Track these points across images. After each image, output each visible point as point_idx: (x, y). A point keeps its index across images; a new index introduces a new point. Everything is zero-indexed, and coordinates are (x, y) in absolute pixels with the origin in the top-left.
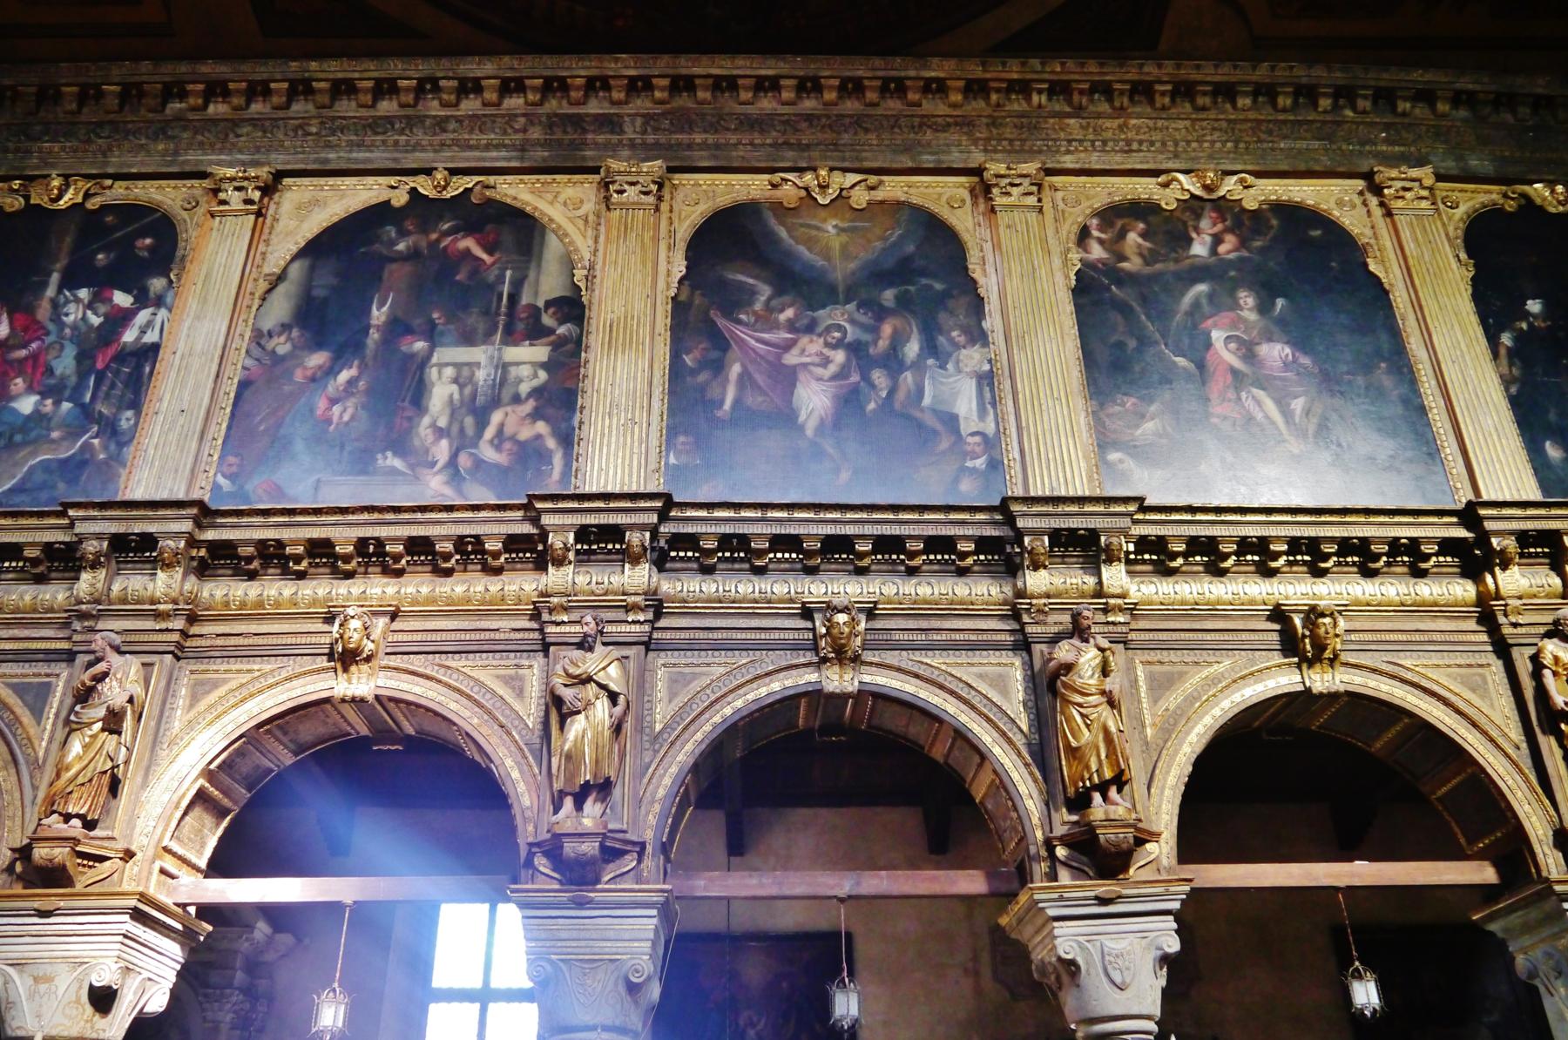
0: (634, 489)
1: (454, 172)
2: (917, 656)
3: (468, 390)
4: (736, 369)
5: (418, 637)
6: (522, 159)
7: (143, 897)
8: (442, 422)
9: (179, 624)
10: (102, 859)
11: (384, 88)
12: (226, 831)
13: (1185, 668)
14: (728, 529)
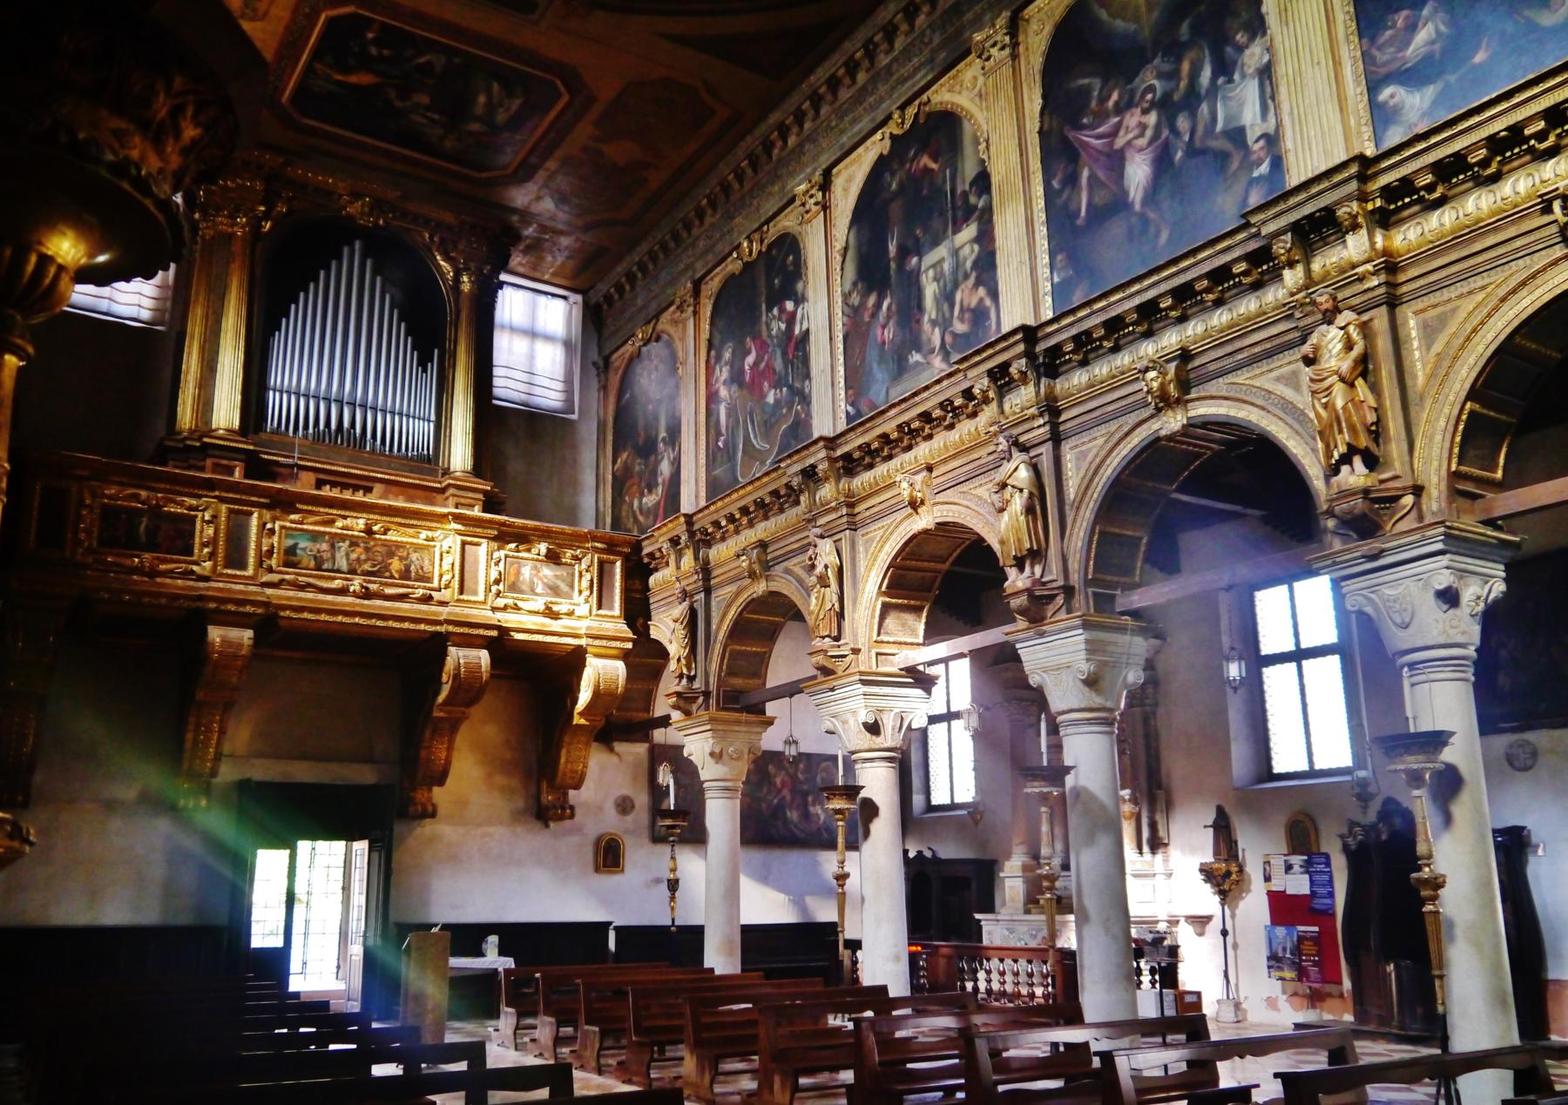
0: (1323, 168)
1: (902, 108)
2: (1230, 378)
3: (941, 283)
4: (1085, 173)
5: (950, 475)
6: (932, 69)
7: (861, 673)
8: (933, 316)
9: (844, 511)
10: (845, 656)
11: (852, 67)
12: (927, 617)
13: (1458, 303)
14: (1074, 331)
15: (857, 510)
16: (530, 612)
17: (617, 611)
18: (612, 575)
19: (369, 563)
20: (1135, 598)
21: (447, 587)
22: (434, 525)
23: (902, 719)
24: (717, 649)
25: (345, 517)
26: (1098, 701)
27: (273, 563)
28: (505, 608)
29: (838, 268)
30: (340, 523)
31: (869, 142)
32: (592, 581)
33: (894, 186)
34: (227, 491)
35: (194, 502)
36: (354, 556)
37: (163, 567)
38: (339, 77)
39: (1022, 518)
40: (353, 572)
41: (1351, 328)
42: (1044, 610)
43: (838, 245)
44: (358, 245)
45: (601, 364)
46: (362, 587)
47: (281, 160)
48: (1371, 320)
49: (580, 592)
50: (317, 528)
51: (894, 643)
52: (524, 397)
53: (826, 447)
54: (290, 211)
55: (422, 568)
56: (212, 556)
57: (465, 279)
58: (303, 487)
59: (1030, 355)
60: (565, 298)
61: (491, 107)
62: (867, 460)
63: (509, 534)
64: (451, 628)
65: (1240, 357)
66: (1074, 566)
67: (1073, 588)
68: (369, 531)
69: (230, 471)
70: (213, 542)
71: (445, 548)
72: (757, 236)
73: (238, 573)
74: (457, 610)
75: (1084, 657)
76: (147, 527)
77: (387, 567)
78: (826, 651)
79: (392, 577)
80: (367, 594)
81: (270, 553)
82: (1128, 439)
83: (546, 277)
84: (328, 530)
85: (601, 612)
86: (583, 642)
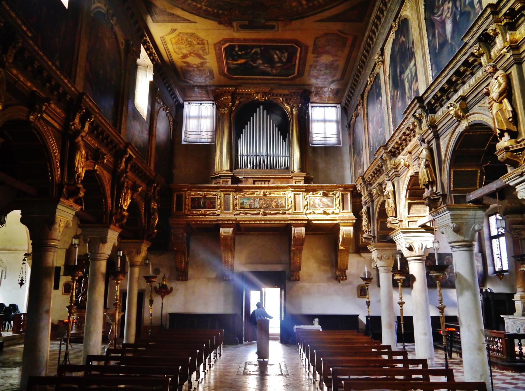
1: (394, 21)
4: (437, 32)
5: (415, 155)
7: (401, 229)
9: (393, 170)
10: (397, 223)
15: (399, 169)
16: (319, 214)
17: (350, 210)
18: (347, 198)
19: (266, 204)
20: (471, 196)
21: (291, 208)
22: (285, 190)
23: (422, 244)
24: (376, 222)
25: (257, 192)
26: (461, 238)
27: (238, 207)
28: (310, 213)
29: (388, 82)
30: (256, 193)
31: (390, 36)
32: (340, 201)
33: (397, 50)
34: (223, 189)
35: (214, 193)
36: (261, 203)
37: (208, 213)
38: (235, 63)
39: (425, 170)
40: (261, 208)
41: (499, 78)
42: (437, 204)
43: (387, 74)
44: (261, 107)
45: (348, 126)
46: (263, 212)
47: (234, 89)
48: (511, 72)
49: (336, 205)
50: (249, 196)
51: (416, 217)
52: (323, 142)
53: (384, 149)
54: (240, 103)
55: (282, 204)
56: (220, 207)
57: (294, 110)
58: (249, 184)
59: (422, 107)
60: (336, 107)
61: (280, 58)
62: (397, 151)
63: (310, 190)
64: (292, 222)
65: (480, 95)
66: (446, 186)
67: (446, 195)
68: (264, 195)
69: (227, 182)
70: (221, 203)
71: (289, 197)
72: (371, 76)
73: (228, 212)
74: (294, 216)
75: (451, 221)
76: (203, 202)
77: (271, 205)
78: (390, 222)
79: (273, 208)
80: (265, 214)
81: (236, 205)
82: (454, 134)
83: (326, 102)
84: (252, 196)
85: (344, 211)
86: (337, 222)
